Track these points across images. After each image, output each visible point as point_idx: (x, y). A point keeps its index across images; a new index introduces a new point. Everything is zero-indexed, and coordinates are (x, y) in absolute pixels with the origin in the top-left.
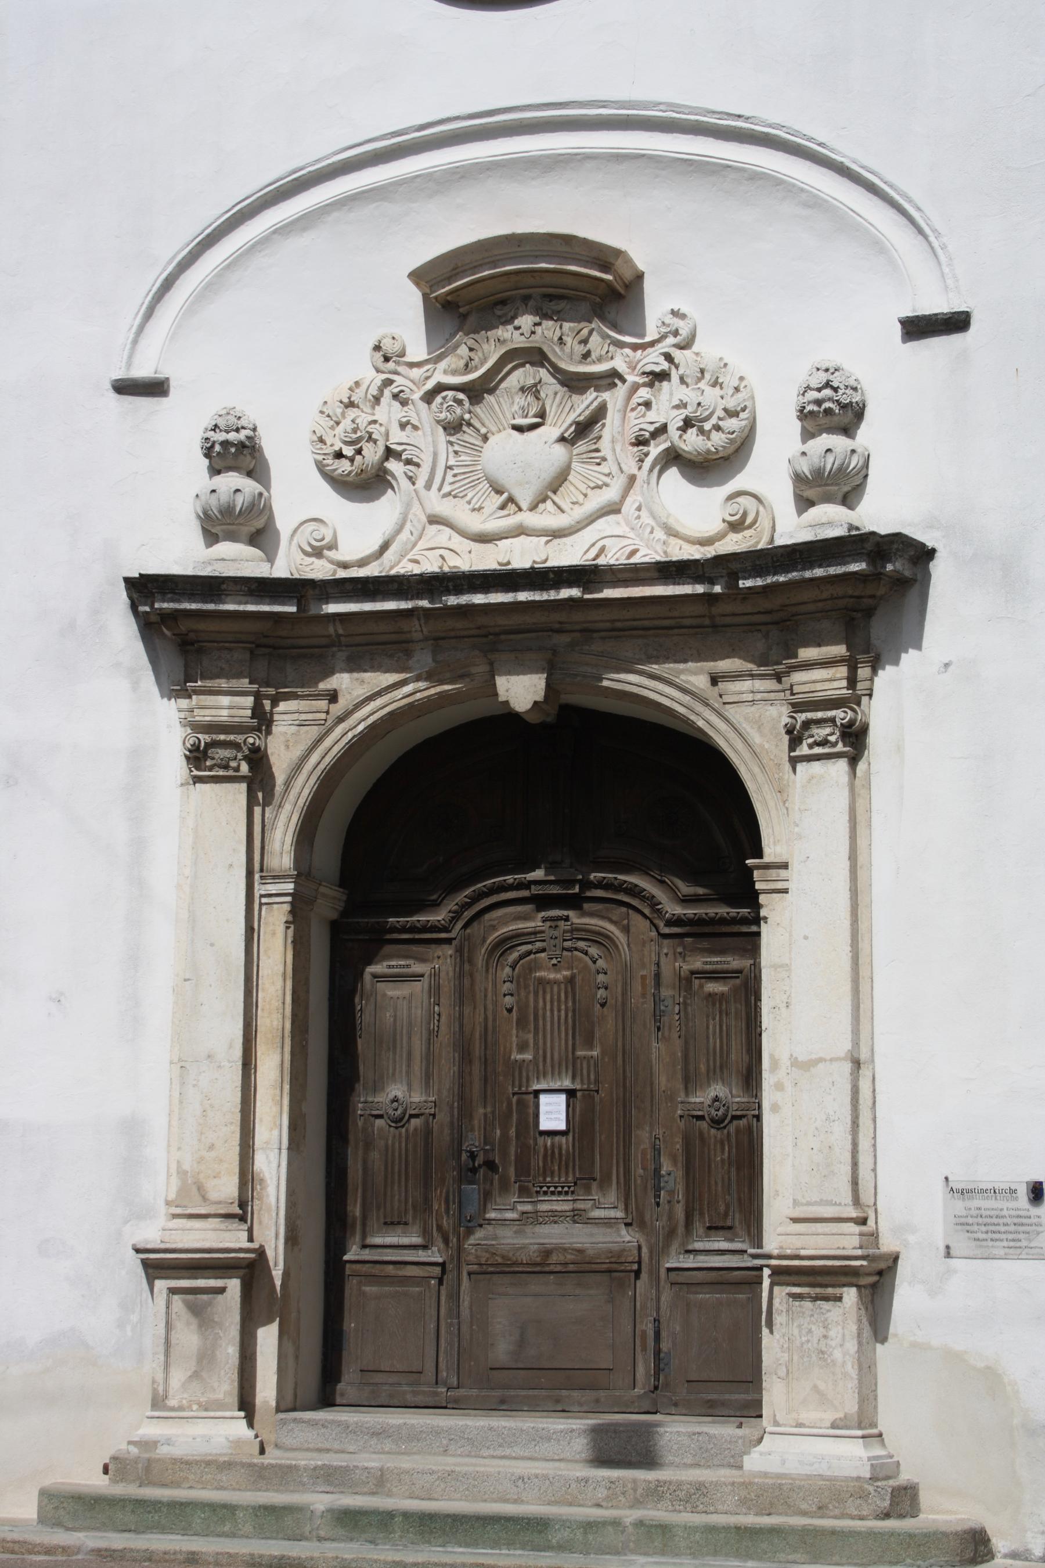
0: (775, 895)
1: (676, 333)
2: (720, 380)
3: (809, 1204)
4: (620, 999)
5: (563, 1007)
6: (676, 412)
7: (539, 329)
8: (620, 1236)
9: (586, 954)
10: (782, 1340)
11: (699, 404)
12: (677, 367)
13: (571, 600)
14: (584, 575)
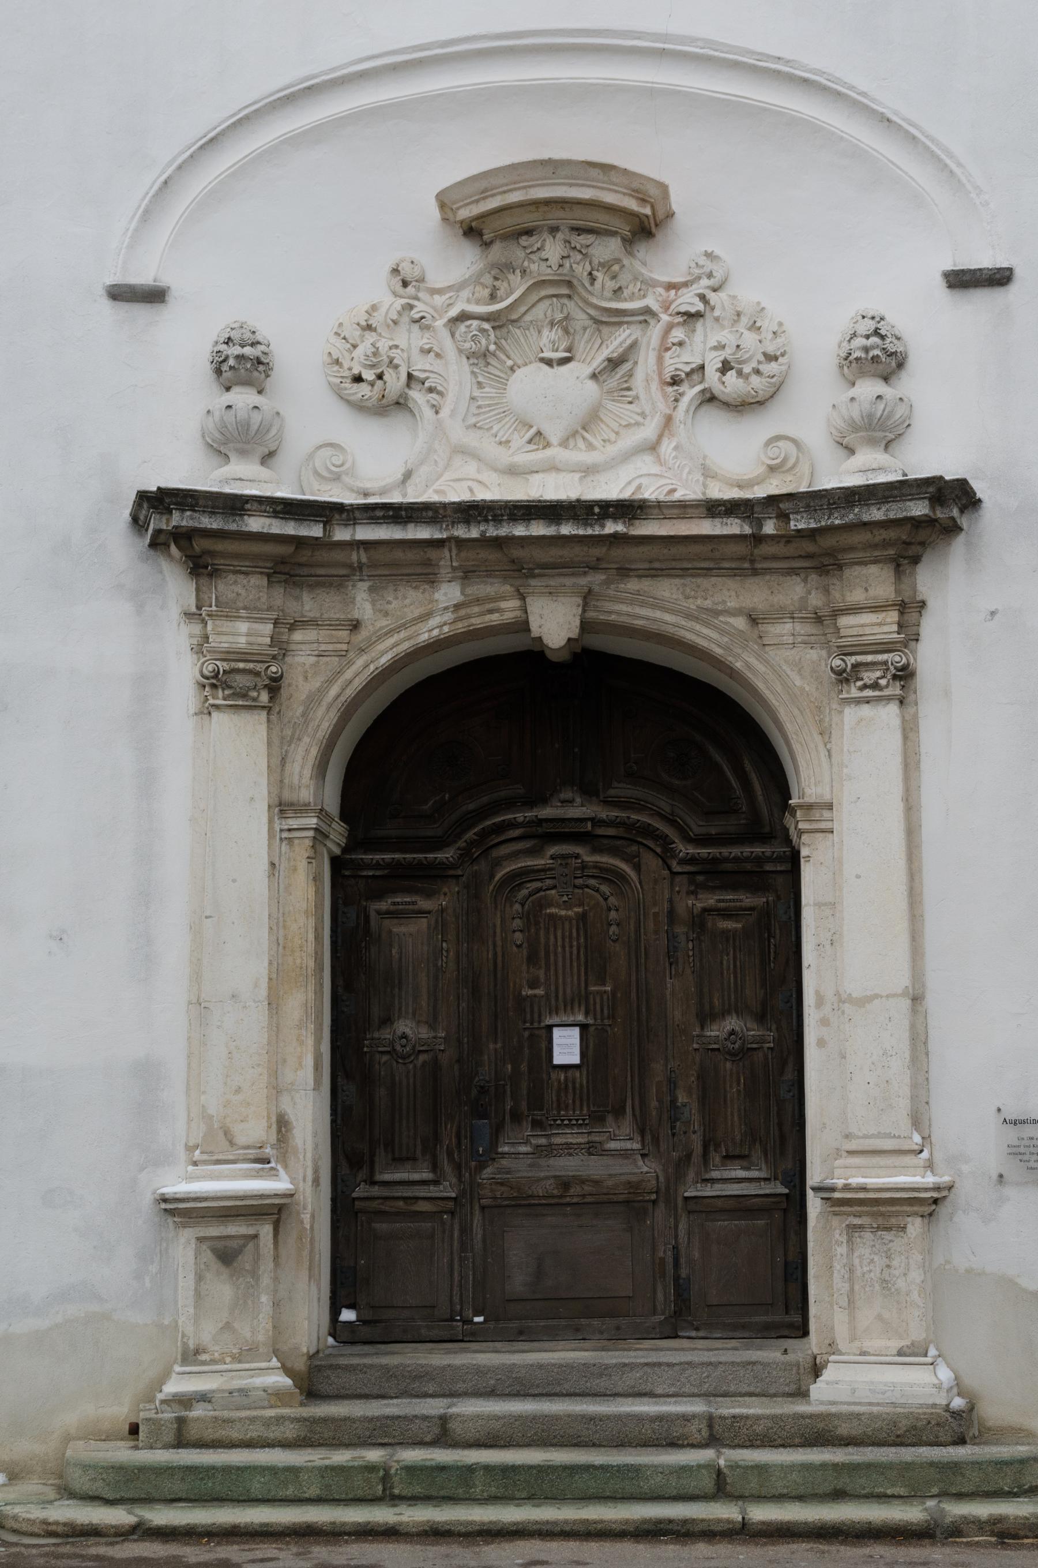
0: (818, 835)
1: (710, 275)
2: (758, 324)
3: (865, 1137)
4: (632, 935)
5: (575, 943)
6: (715, 354)
7: (567, 263)
8: (637, 1166)
9: (597, 891)
10: (843, 1271)
11: (738, 346)
12: (713, 309)
13: (615, 536)
14: (628, 509)
